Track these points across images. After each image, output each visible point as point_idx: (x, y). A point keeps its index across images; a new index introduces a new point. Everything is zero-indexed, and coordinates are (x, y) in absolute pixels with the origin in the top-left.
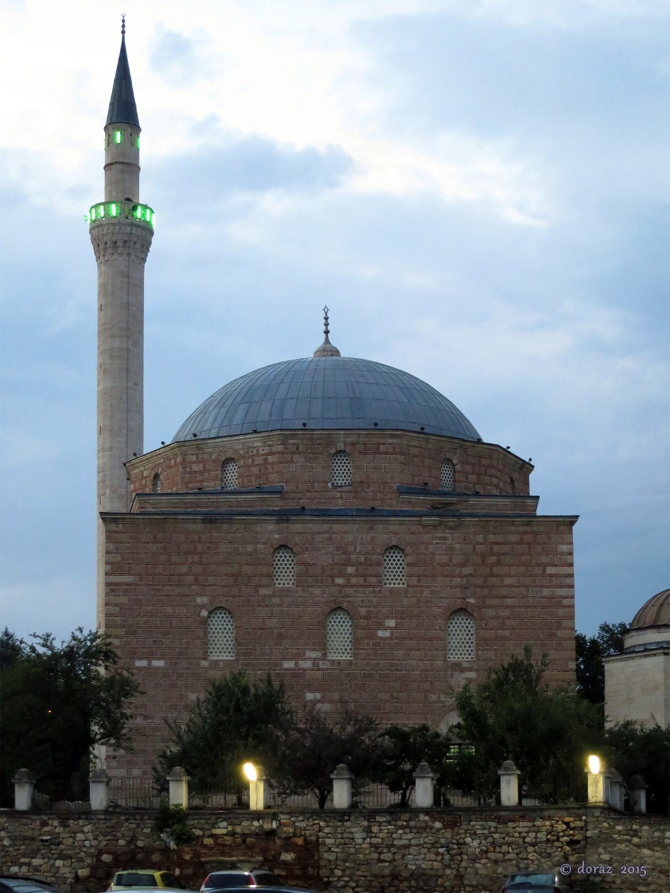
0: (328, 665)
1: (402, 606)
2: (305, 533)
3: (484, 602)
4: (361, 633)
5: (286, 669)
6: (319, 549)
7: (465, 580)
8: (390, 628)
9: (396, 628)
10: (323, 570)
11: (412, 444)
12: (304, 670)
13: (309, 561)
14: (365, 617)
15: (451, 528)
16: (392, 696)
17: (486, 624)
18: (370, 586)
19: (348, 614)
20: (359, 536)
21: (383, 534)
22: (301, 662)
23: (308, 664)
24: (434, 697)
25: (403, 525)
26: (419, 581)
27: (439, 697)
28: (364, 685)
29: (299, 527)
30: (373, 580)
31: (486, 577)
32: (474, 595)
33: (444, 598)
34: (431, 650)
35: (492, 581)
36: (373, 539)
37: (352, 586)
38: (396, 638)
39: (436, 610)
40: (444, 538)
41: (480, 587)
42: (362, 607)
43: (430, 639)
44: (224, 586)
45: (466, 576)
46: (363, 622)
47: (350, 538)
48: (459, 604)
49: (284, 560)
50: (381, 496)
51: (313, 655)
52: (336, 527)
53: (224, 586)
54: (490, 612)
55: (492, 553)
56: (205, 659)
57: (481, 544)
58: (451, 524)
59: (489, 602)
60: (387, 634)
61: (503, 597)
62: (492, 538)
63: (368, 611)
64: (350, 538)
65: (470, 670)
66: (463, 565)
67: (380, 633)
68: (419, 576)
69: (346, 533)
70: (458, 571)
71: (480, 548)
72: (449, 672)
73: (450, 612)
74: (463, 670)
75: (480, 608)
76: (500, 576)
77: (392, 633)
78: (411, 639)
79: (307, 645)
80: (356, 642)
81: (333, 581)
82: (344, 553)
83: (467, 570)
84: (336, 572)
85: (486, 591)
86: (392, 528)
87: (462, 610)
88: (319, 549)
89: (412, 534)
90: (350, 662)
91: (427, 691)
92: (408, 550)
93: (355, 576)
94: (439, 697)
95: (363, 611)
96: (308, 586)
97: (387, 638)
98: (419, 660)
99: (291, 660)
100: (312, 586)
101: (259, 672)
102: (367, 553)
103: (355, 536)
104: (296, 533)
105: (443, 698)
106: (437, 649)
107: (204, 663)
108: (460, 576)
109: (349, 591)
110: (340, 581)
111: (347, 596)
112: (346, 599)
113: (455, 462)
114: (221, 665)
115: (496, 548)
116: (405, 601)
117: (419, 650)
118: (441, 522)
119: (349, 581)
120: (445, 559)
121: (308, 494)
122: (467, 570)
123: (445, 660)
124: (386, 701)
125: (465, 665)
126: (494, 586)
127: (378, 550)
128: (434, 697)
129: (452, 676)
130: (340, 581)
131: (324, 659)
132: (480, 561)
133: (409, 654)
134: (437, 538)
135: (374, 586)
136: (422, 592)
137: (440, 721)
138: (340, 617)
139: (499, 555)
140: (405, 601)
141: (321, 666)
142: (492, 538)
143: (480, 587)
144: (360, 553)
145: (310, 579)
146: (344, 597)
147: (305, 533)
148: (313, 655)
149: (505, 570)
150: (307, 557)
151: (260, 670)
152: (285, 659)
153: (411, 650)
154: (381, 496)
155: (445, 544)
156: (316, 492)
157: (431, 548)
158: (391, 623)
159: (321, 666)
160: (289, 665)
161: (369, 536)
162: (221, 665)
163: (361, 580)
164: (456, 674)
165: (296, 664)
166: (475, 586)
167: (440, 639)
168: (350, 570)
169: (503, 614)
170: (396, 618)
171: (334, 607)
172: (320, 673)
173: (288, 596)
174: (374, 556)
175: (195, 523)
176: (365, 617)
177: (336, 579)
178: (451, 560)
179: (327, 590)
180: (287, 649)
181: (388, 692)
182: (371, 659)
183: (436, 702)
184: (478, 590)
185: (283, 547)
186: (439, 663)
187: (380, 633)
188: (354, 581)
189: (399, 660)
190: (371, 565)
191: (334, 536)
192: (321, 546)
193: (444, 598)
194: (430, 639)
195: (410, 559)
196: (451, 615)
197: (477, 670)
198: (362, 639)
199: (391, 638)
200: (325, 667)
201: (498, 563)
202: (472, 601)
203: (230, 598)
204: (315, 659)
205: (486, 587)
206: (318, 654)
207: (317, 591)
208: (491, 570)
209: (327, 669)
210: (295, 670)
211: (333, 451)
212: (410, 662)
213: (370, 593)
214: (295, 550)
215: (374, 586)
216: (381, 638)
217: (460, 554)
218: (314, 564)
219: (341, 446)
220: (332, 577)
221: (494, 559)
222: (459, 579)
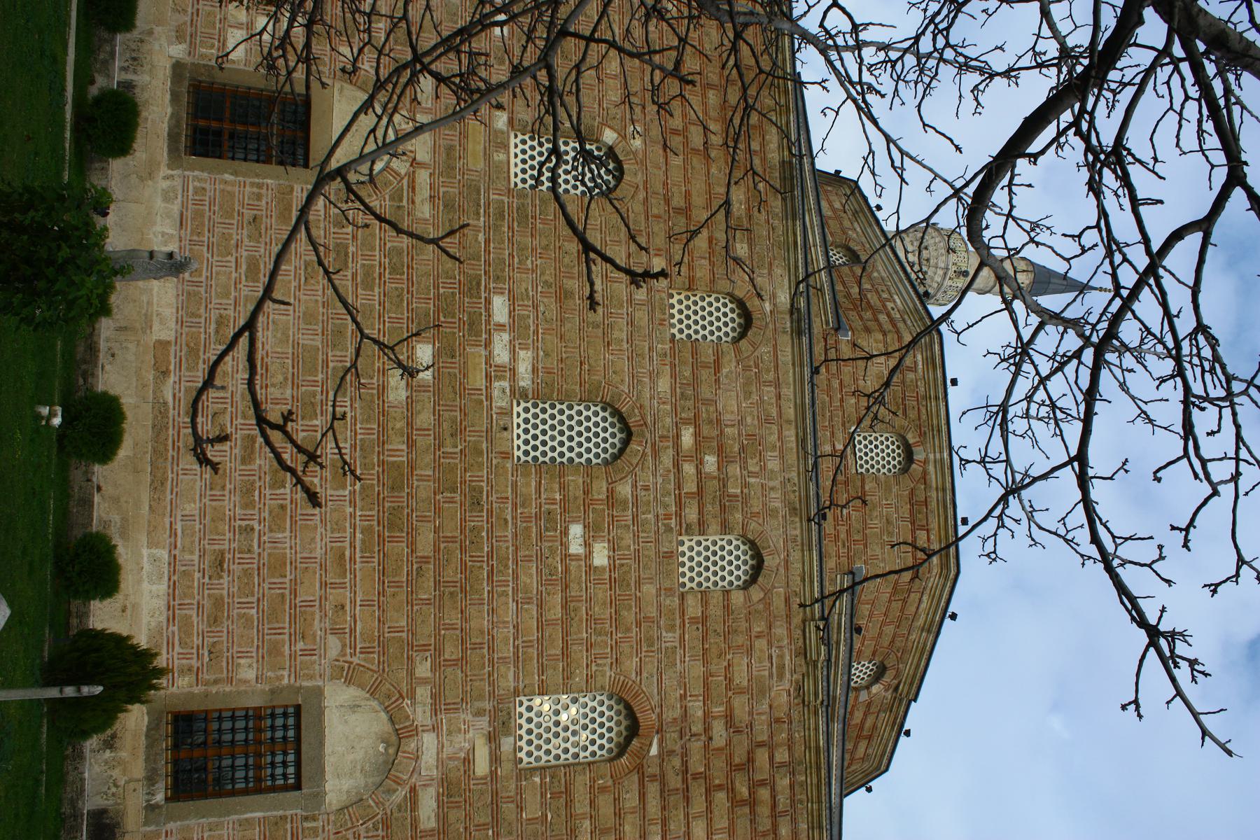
0: (500, 402)
1: (639, 583)
2: (776, 367)
3: (653, 778)
4: (575, 481)
5: (488, 302)
6: (748, 395)
7: (697, 728)
8: (589, 555)
9: (590, 568)
10: (707, 402)
11: (925, 598)
12: (488, 344)
13: (725, 371)
14: (611, 493)
15: (799, 688)
16: (425, 560)
17: (603, 789)
18: (680, 505)
19: (616, 457)
20: (776, 483)
21: (780, 535)
22: (506, 337)
23: (501, 355)
24: (423, 669)
25: (803, 580)
26: (694, 620)
27: (424, 681)
28: (454, 490)
29: (786, 355)
30: (691, 514)
31: (705, 776)
32: (665, 754)
33: (660, 681)
34: (540, 655)
35: (698, 791)
36: (773, 513)
37: (677, 465)
38: (567, 570)
39: (631, 664)
40: (781, 676)
41: (685, 764)
42: (635, 486)
43: (566, 653)
44: (665, 184)
45: (707, 729)
46: (600, 489)
47: (773, 465)
48: (647, 719)
49: (723, 319)
50: (843, 536)
51: (524, 368)
52: (790, 434)
53: (665, 184)
54: (631, 799)
55: (754, 786)
56: (511, 122)
57: (771, 758)
58: (809, 686)
59: (653, 789)
60: (576, 548)
61: (664, 822)
62: (783, 782)
63: (625, 502)
64: (773, 465)
65: (495, 759)
66: (729, 718)
67: (576, 530)
68: (704, 619)
69: (782, 457)
70: (718, 710)
71: (762, 756)
72: (487, 705)
73: (628, 698)
74: (492, 738)
75: (640, 769)
76: (709, 810)
77: (577, 558)
78: (565, 606)
79: (547, 355)
80: (557, 470)
81: (686, 422)
82: (743, 449)
83: (719, 733)
84: (706, 430)
85: (675, 782)
86: (796, 555)
87: (633, 728)
88: (748, 395)
89: (787, 600)
90: (507, 455)
91: (439, 651)
92: (756, 593)
93: (699, 472)
94: (424, 681)
95: (625, 490)
96: (673, 366)
97: (565, 545)
98: (516, 627)
99: (511, 313)
100: (674, 376)
101: (481, 237)
102: (745, 500)
103: (773, 477)
104: (775, 346)
105: (423, 693)
106: (542, 670)
107: (501, 120)
108: (706, 715)
109: (667, 459)
110: (687, 438)
111: (656, 453)
112: (648, 450)
113: (875, 689)
114: (499, 157)
115: (764, 793)
116: (649, 589)
117: (541, 627)
118: (815, 664)
119: (689, 458)
120: (741, 678)
121: (836, 383)
122: (719, 729)
123: (516, 693)
124: (412, 546)
125: (507, 743)
126: (687, 800)
127: (753, 525)
128: (423, 669)
129: (479, 713)
130: (687, 438)
131: (513, 392)
132: (737, 760)
133: (528, 601)
134: (781, 657)
135: (679, 515)
136: (671, 628)
137: (361, 686)
138: (611, 437)
139: (752, 803)
140: (649, 589)
141: (496, 384)
142: (783, 782)
143: (685, 764)
144: (746, 485)
145: (687, 373)
146: (654, 445)
147: (776, 367)
148: (524, 368)
149: (722, 823)
150: (729, 366)
151: (487, 241)
152: (512, 299)
153: (540, 606)
154: (843, 536)
155: (771, 675)
156: (842, 400)
157: (761, 644)
158: (600, 557)
159: (496, 384)
160: (500, 308)
161: (778, 504)
162: (499, 157)
163: (690, 487)
164: (484, 723)
165: (501, 327)
166: (685, 754)
167: (568, 676)
168: (711, 461)
169: (627, 828)
170: (613, 567)
171: (632, 421)
172: (481, 382)
173: (651, 320)
174: (739, 516)
175: (781, 147)
176: (611, 493)
177: (691, 430)
178: (741, 692)
179: (668, 407)
180: (535, 307)
181: (436, 550)
182: (515, 506)
183: (411, 673)
184: (677, 762)
185: (747, 319)
186: (508, 680)
187: (576, 530)
188: (689, 469)
189: (516, 577)
190: (723, 509)
191: (775, 428)
192: (755, 397)
193: (660, 681)
194: (566, 653)
195: (738, 598)
196: (620, 700)
197: (493, 773)
198: (562, 487)
199: (566, 556)
200: (496, 393)
201: (735, 802)
202: (654, 751)
203: (642, 195)
204: (513, 371)
205: (685, 781)
206: (525, 381)
207: (664, 385)
208: (720, 787)
209: (490, 398)
210: (488, 322)
211: (911, 438)
212: (512, 606)
213: (666, 506)
214: (743, 343)
215: (679, 515)
216: (565, 532)
217: (751, 713)
218: (717, 381)
219: (919, 455)
220: (695, 422)
221: (744, 791)
222: (700, 713)
